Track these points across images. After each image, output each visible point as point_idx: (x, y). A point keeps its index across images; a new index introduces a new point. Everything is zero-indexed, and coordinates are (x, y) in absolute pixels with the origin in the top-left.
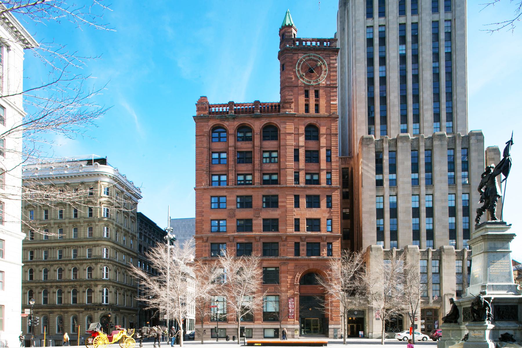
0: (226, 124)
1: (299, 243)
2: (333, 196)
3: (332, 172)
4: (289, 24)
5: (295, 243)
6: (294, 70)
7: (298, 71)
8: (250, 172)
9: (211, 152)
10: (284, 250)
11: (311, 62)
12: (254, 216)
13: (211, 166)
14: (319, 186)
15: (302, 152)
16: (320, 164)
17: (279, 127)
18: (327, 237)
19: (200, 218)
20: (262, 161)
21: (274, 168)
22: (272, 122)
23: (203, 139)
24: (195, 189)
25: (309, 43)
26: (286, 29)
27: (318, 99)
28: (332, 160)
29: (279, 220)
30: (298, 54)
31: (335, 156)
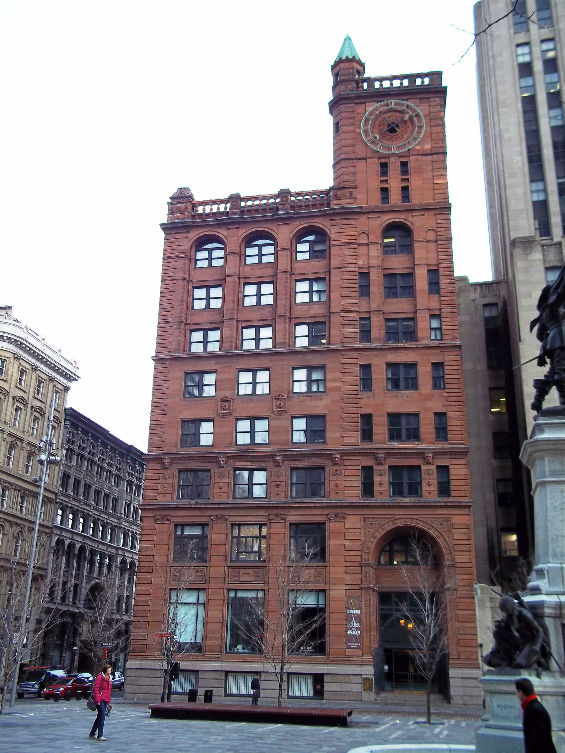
0: (222, 233)
1: (371, 468)
2: (446, 363)
3: (443, 315)
4: (347, 57)
5: (363, 468)
6: (358, 131)
7: (366, 132)
8: (269, 323)
9: (191, 288)
10: (336, 485)
11: (392, 113)
12: (273, 412)
13: (189, 312)
14: (417, 343)
15: (375, 277)
16: (416, 299)
17: (328, 232)
18: (437, 454)
19: (160, 418)
20: (293, 299)
21: (317, 312)
22: (314, 224)
23: (175, 264)
24: (154, 359)
25: (386, 84)
26: (342, 65)
27: (406, 177)
28: (442, 291)
29: (328, 418)
30: (365, 103)
31: (447, 282)
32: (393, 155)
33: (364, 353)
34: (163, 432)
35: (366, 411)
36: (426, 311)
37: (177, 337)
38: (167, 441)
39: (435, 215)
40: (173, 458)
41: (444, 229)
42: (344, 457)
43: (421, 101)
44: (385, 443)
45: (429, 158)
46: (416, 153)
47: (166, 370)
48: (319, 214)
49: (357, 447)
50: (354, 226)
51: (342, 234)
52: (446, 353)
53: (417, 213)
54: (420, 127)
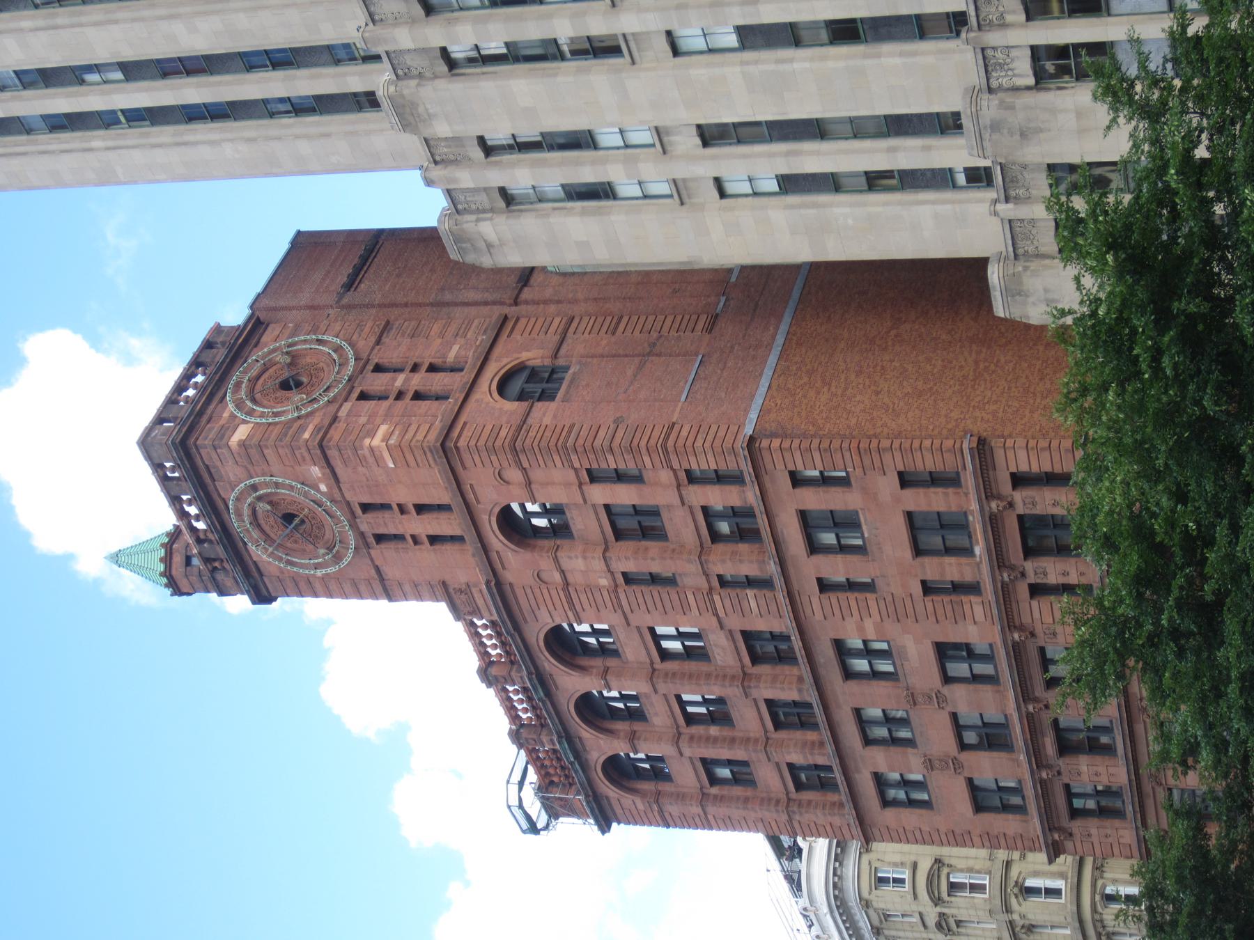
7: (316, 567)
9: (714, 790)
11: (262, 522)
18: (988, 491)
22: (542, 644)
32: (354, 525)
33: (795, 586)
34: (1002, 835)
35: (917, 590)
36: (683, 492)
37: (817, 815)
38: (1020, 831)
39: (464, 468)
40: (1050, 830)
41: (494, 458)
42: (1017, 623)
43: (216, 478)
44: (978, 565)
45: (338, 471)
46: (336, 490)
47: (884, 830)
48: (519, 641)
49: (994, 605)
50: (529, 591)
51: (551, 608)
52: (769, 466)
53: (471, 497)
54: (277, 485)
